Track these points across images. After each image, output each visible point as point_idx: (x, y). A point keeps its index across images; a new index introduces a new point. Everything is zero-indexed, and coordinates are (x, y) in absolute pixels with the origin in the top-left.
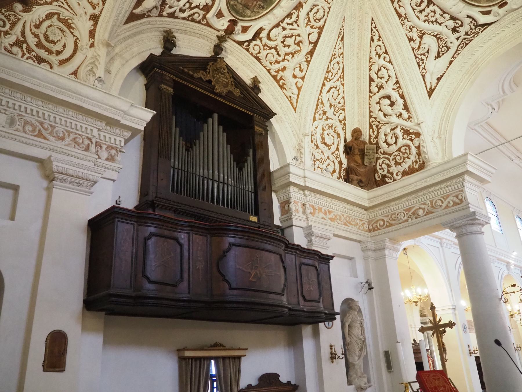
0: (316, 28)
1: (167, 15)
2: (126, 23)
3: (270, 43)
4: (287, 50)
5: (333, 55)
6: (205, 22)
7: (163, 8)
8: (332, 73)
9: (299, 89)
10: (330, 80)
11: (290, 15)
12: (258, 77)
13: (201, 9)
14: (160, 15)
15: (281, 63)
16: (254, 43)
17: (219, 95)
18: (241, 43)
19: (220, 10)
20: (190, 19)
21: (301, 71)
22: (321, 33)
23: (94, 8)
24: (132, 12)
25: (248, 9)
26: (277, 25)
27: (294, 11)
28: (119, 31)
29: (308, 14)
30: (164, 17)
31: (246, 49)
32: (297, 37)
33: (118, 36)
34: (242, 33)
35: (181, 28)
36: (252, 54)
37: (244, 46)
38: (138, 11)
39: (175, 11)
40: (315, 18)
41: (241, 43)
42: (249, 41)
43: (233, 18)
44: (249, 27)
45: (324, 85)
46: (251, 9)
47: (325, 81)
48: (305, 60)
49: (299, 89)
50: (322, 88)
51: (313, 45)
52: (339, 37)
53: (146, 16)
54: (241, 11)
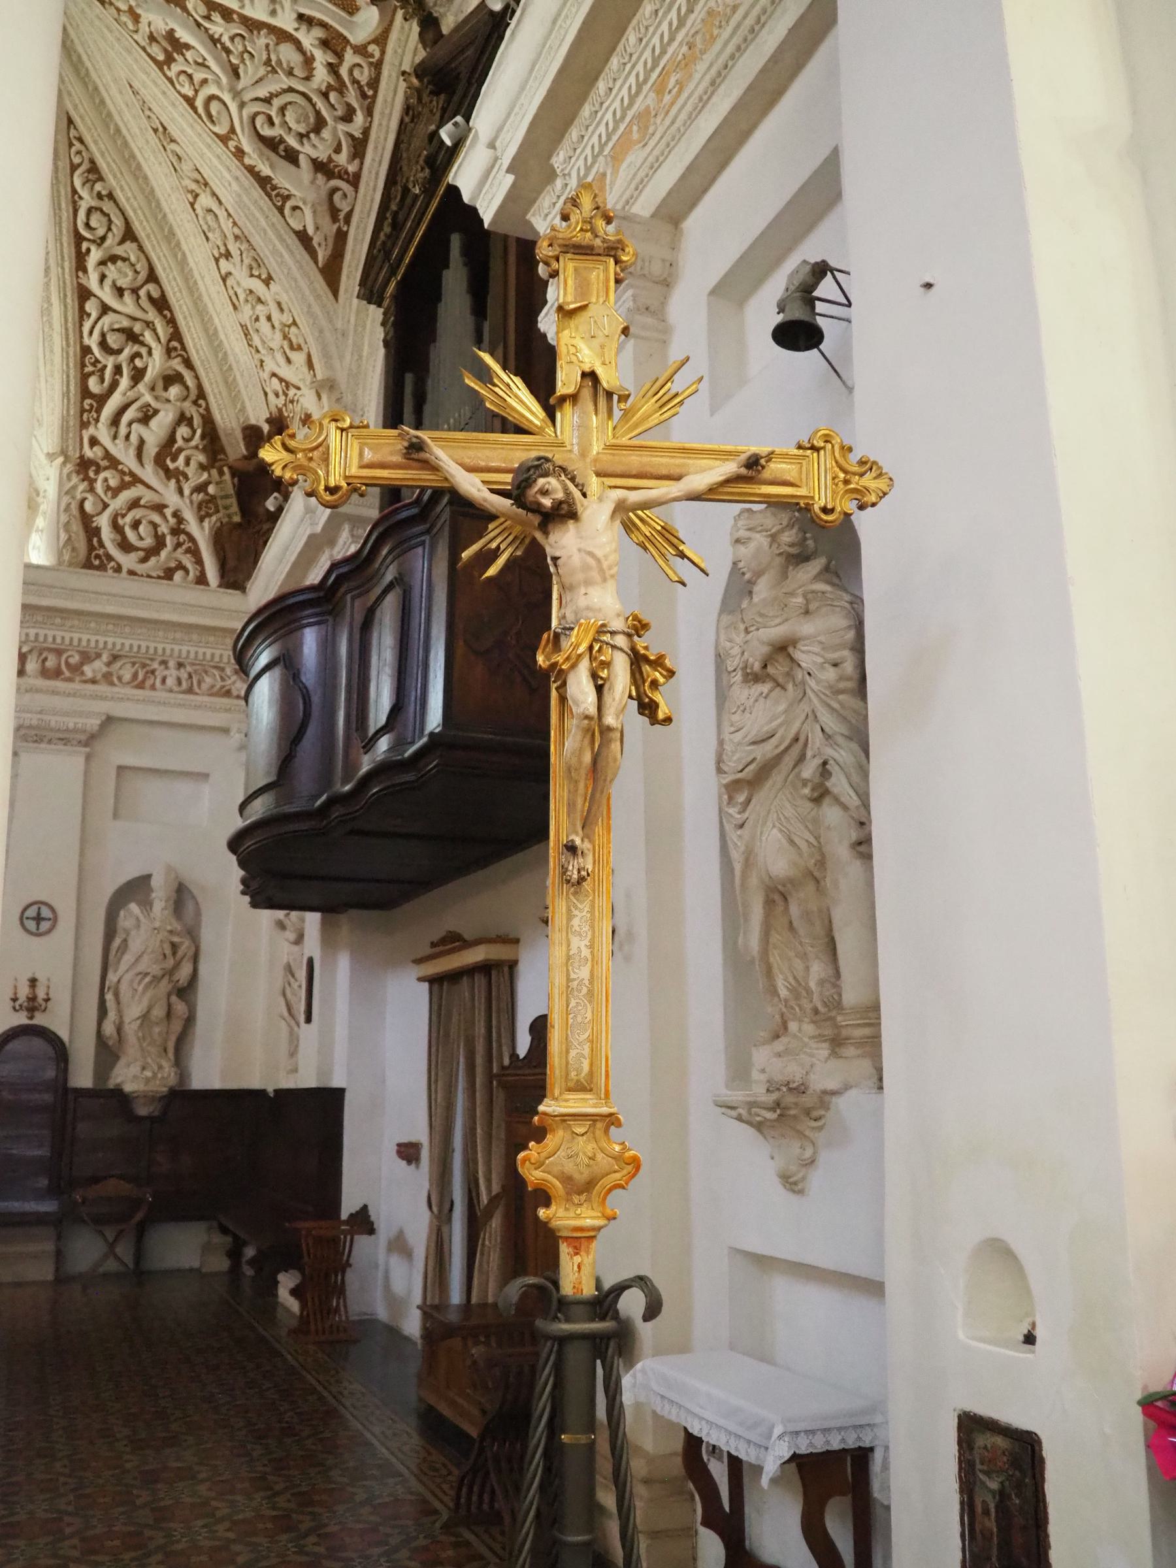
1: (357, 161)
6: (373, 49)
7: (339, 172)
20: (370, 93)
30: (361, 169)
38: (322, 255)
39: (352, 136)
53: (345, 229)
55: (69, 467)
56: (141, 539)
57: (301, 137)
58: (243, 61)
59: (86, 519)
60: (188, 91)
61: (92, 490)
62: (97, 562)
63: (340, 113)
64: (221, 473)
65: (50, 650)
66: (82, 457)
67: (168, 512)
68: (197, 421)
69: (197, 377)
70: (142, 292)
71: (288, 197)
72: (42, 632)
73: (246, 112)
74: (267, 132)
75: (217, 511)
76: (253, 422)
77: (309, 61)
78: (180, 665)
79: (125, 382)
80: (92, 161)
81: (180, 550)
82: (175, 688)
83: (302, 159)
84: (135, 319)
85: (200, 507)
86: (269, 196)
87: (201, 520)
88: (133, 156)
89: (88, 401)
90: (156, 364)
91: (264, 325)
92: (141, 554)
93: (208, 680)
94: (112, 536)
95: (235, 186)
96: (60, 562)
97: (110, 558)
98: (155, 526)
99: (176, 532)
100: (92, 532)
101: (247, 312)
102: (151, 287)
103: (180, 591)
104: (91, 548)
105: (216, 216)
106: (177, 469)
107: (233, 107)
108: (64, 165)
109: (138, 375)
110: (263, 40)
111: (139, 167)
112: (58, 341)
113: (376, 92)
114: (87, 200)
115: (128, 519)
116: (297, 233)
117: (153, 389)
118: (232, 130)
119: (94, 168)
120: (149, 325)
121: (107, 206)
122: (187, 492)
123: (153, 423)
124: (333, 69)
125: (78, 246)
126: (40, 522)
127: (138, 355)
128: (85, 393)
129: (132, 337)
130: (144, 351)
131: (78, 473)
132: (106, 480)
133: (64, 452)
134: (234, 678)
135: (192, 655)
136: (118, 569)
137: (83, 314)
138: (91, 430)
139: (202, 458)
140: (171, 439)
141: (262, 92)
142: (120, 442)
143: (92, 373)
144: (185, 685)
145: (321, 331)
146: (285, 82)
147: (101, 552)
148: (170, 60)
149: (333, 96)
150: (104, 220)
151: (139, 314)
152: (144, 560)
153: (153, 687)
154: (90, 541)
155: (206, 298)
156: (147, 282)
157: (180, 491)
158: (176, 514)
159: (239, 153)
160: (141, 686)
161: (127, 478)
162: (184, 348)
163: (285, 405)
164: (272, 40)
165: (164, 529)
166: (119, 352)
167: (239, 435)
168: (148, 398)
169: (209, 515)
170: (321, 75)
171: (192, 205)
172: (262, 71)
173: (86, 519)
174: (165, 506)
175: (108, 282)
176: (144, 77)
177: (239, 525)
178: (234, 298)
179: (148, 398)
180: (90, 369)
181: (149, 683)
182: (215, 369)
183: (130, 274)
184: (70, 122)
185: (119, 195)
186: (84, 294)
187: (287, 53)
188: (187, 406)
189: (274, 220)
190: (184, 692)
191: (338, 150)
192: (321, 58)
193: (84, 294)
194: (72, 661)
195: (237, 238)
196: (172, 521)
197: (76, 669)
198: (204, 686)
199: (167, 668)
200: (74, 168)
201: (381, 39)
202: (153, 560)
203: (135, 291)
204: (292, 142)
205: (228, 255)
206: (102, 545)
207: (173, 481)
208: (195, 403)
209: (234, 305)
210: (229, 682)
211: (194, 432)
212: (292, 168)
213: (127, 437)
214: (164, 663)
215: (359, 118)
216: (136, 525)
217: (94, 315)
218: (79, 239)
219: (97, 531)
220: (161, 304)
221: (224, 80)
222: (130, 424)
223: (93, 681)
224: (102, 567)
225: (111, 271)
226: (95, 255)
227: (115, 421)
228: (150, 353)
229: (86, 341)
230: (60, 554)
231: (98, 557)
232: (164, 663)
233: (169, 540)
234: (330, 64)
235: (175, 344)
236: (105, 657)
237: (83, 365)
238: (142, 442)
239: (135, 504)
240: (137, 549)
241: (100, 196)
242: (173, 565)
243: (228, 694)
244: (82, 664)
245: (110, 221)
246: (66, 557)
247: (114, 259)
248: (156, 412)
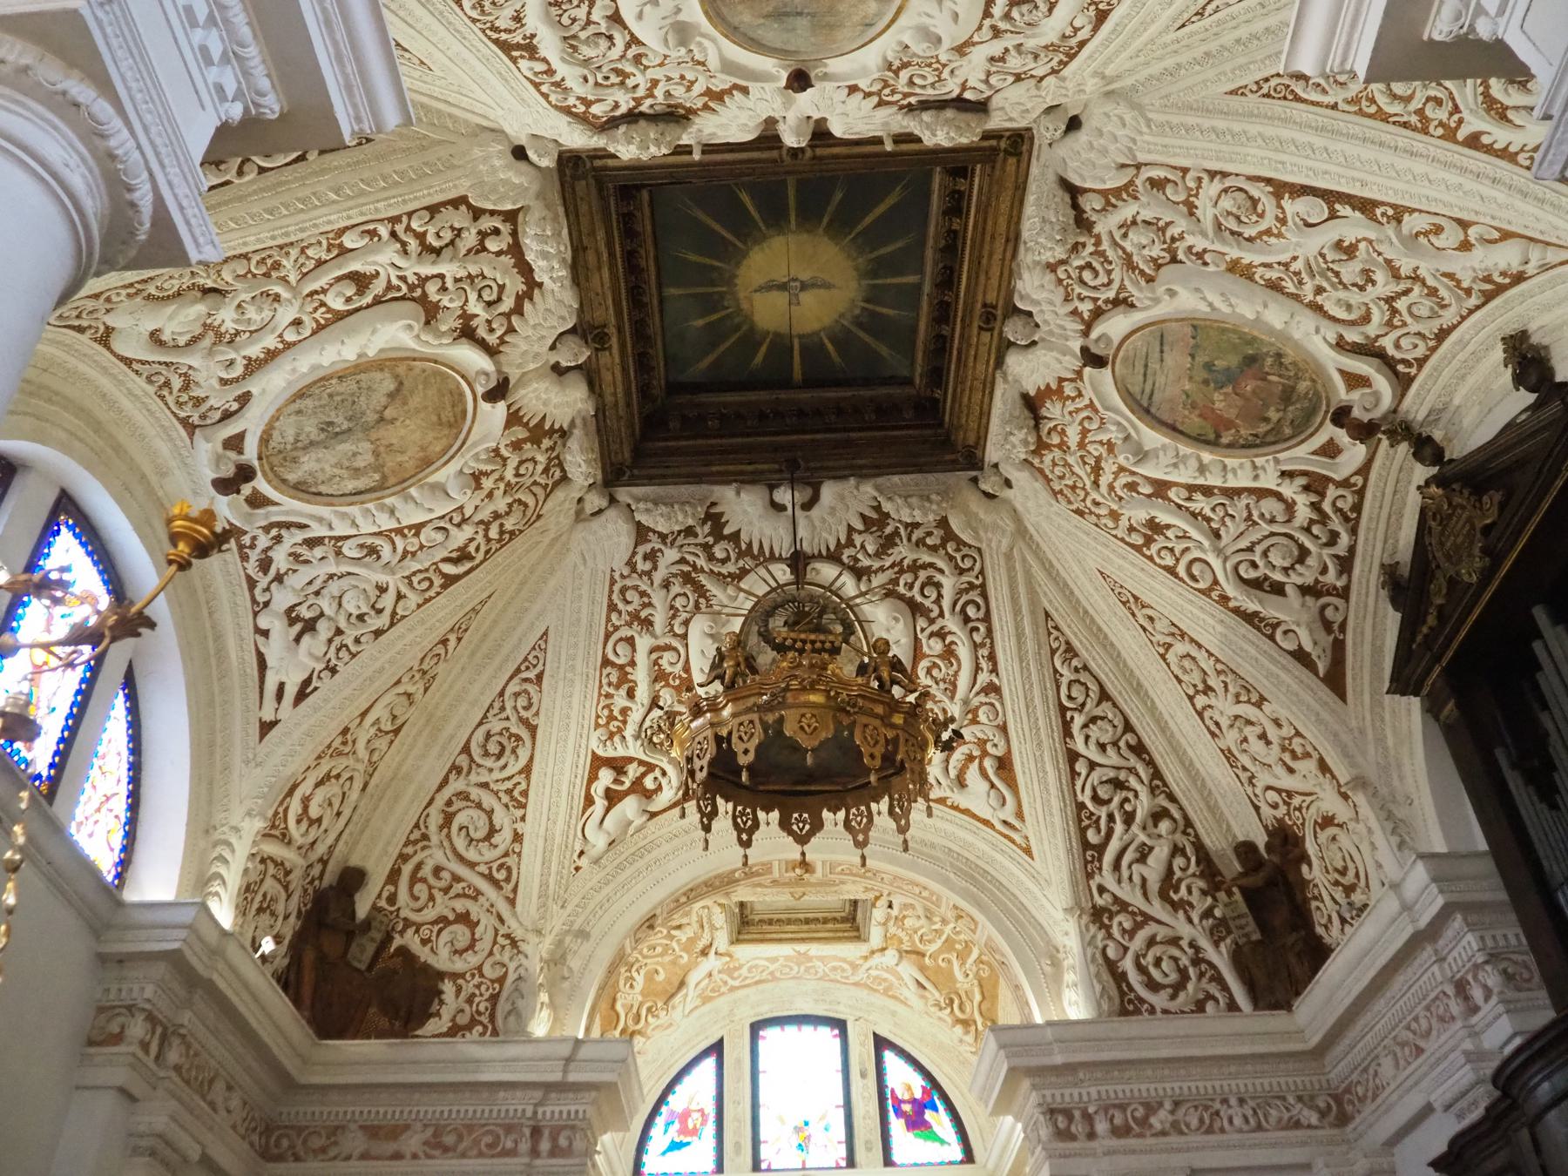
0: (1280, 206)
1: (1345, 577)
2: (1342, 696)
3: (1377, 317)
4: (1380, 276)
5: (1361, 113)
8: (1428, 99)
9: (1506, 235)
10: (1456, 109)
11: (1274, 286)
12: (1509, 331)
13: (1322, 495)
14: (1344, 594)
15: (1430, 282)
16: (1391, 351)
17: (1487, 576)
18: (1403, 383)
19: (1314, 453)
21: (1438, 230)
22: (1293, 185)
23: (1307, 755)
24: (1322, 680)
25: (1293, 388)
26: (1318, 308)
27: (1257, 277)
28: (1354, 724)
29: (1250, 240)
30: (1350, 581)
31: (1420, 367)
32: (1329, 258)
33: (1362, 732)
34: (1370, 386)
35: (1380, 535)
36: (1433, 350)
37: (1413, 371)
39: (1337, 557)
40: (1254, 218)
41: (1403, 383)
42: (1388, 363)
43: (1328, 421)
44: (1341, 372)
45: (1474, 141)
46: (1291, 383)
47: (1461, 136)
48: (1394, 223)
49: (1506, 235)
50: (1489, 150)
51: (1337, 206)
52: (1298, 99)
54: (1306, 404)
55: (1085, 918)
56: (1166, 975)
57: (1286, 570)
58: (1224, 524)
59: (1111, 966)
60: (1169, 561)
61: (1110, 936)
62: (1131, 1008)
63: (1324, 540)
64: (1230, 894)
65: (1115, 1106)
66: (1094, 907)
67: (1184, 943)
68: (1189, 850)
69: (1181, 808)
70: (1122, 744)
71: (1278, 624)
72: (1103, 1089)
73: (1229, 565)
74: (1253, 575)
75: (1229, 932)
76: (1241, 838)
77: (1290, 507)
78: (1242, 1101)
79: (1119, 827)
80: (1068, 643)
81: (1204, 980)
82: (1245, 1128)
83: (1288, 589)
84: (1119, 768)
85: (1212, 934)
86: (1259, 629)
87: (1216, 944)
88: (1100, 629)
89: (1089, 853)
90: (1143, 805)
91: (1256, 746)
92: (1170, 991)
93: (1273, 1112)
94: (1140, 978)
95: (1219, 628)
96: (1100, 1015)
97: (1142, 1001)
98: (1175, 960)
99: (1196, 962)
100: (1120, 978)
101: (1230, 738)
102: (1129, 737)
103: (1214, 1021)
104: (1122, 994)
105: (1194, 659)
106: (1181, 900)
107: (1216, 563)
108: (1046, 651)
109: (1129, 819)
110: (1245, 500)
111: (1106, 637)
112: (1056, 804)
113: (1359, 514)
114: (1067, 675)
115: (1150, 958)
116: (1293, 654)
117: (1144, 828)
118: (1216, 582)
119: (1070, 651)
120: (1132, 770)
121: (1084, 677)
122: (1196, 920)
123: (1151, 860)
124: (1315, 507)
125: (1063, 716)
126: (1069, 977)
127: (1126, 800)
128: (1086, 845)
129: (1118, 784)
130: (1131, 795)
131: (1094, 922)
132: (1120, 924)
133: (1078, 903)
134: (1299, 1106)
135: (1250, 1088)
136: (1152, 1011)
137: (1074, 774)
138: (1097, 879)
139: (1201, 884)
140: (1170, 871)
141: (1244, 544)
142: (1125, 884)
143: (1089, 826)
144: (1252, 1121)
145: (1336, 735)
146: (1266, 528)
147: (1132, 996)
148: (1149, 541)
149: (1316, 530)
150: (1083, 689)
151: (1122, 763)
152: (1173, 997)
153: (1222, 1130)
154: (1119, 988)
155: (1178, 735)
156: (1124, 733)
157: (1190, 921)
158: (1192, 944)
159: (1224, 599)
160: (1210, 1131)
161: (1139, 919)
162: (1165, 785)
163: (1288, 814)
164: (1251, 500)
165: (1185, 961)
166: (1110, 801)
167: (1233, 857)
168: (1142, 837)
169: (1223, 939)
170: (1303, 513)
171: (1163, 657)
172: (1243, 527)
173: (1111, 966)
174: (1180, 938)
175: (1092, 741)
176: (1121, 562)
177: (1259, 942)
178: (1213, 728)
179: (1142, 837)
180: (1087, 822)
181: (1217, 1125)
182: (1196, 796)
183: (1110, 729)
184: (1047, 615)
185: (1092, 665)
186: (1073, 757)
187: (1270, 506)
188: (1179, 838)
189: (1265, 647)
190: (1253, 1131)
191: (1324, 571)
192: (1302, 502)
193: (1073, 757)
194: (1138, 1114)
195: (1219, 673)
196: (1190, 951)
197: (1144, 1122)
198: (1273, 1120)
199: (1230, 1107)
200: (1053, 652)
201: (1364, 470)
202: (1182, 996)
203: (1115, 744)
204: (1278, 576)
205: (1208, 689)
206: (1131, 989)
207: (1181, 913)
208: (1184, 833)
209: (1213, 735)
210: (1295, 1112)
211: (1188, 860)
212: (1280, 599)
213: (1130, 878)
214: (1225, 1101)
215: (1344, 539)
216: (1158, 962)
217: (1084, 772)
218: (1063, 710)
219: (1124, 975)
220: (1139, 749)
221: (1206, 543)
222: (1130, 867)
223: (1163, 1133)
224: (1137, 1012)
225: (1094, 731)
226: (1079, 720)
227: (1117, 866)
228: (1136, 796)
229: (1080, 798)
230: (1099, 1005)
231: (1130, 1001)
232: (1225, 1101)
233: (1191, 971)
234: (1312, 504)
235: (1157, 782)
236: (1168, 1105)
237: (1080, 821)
238: (1144, 880)
239: (1151, 942)
240: (1164, 987)
241: (1077, 670)
242: (1201, 996)
243: (1297, 1125)
244: (1146, 1117)
245: (1087, 689)
246: (1105, 1007)
247: (1094, 720)
248: (1151, 849)
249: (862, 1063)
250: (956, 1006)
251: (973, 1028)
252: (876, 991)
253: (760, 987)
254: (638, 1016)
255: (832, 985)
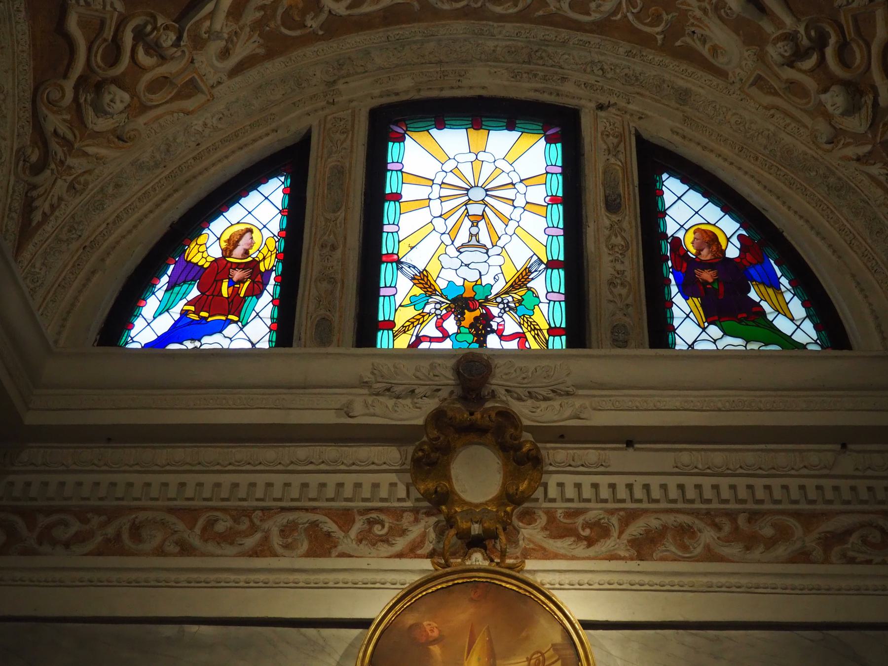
249: (609, 183)
250: (829, 52)
251: (869, 99)
252: (646, 41)
253: (395, 31)
254: (116, 45)
255: (550, 33)
